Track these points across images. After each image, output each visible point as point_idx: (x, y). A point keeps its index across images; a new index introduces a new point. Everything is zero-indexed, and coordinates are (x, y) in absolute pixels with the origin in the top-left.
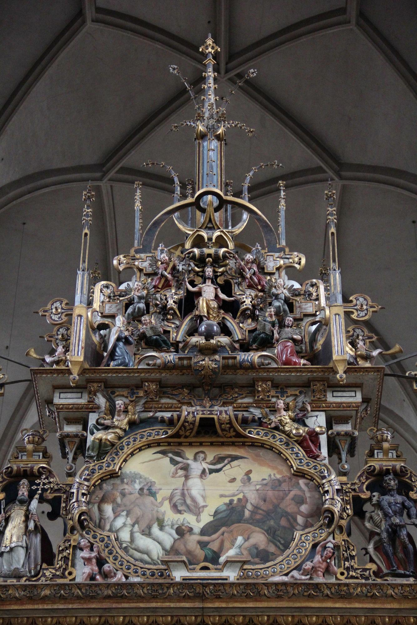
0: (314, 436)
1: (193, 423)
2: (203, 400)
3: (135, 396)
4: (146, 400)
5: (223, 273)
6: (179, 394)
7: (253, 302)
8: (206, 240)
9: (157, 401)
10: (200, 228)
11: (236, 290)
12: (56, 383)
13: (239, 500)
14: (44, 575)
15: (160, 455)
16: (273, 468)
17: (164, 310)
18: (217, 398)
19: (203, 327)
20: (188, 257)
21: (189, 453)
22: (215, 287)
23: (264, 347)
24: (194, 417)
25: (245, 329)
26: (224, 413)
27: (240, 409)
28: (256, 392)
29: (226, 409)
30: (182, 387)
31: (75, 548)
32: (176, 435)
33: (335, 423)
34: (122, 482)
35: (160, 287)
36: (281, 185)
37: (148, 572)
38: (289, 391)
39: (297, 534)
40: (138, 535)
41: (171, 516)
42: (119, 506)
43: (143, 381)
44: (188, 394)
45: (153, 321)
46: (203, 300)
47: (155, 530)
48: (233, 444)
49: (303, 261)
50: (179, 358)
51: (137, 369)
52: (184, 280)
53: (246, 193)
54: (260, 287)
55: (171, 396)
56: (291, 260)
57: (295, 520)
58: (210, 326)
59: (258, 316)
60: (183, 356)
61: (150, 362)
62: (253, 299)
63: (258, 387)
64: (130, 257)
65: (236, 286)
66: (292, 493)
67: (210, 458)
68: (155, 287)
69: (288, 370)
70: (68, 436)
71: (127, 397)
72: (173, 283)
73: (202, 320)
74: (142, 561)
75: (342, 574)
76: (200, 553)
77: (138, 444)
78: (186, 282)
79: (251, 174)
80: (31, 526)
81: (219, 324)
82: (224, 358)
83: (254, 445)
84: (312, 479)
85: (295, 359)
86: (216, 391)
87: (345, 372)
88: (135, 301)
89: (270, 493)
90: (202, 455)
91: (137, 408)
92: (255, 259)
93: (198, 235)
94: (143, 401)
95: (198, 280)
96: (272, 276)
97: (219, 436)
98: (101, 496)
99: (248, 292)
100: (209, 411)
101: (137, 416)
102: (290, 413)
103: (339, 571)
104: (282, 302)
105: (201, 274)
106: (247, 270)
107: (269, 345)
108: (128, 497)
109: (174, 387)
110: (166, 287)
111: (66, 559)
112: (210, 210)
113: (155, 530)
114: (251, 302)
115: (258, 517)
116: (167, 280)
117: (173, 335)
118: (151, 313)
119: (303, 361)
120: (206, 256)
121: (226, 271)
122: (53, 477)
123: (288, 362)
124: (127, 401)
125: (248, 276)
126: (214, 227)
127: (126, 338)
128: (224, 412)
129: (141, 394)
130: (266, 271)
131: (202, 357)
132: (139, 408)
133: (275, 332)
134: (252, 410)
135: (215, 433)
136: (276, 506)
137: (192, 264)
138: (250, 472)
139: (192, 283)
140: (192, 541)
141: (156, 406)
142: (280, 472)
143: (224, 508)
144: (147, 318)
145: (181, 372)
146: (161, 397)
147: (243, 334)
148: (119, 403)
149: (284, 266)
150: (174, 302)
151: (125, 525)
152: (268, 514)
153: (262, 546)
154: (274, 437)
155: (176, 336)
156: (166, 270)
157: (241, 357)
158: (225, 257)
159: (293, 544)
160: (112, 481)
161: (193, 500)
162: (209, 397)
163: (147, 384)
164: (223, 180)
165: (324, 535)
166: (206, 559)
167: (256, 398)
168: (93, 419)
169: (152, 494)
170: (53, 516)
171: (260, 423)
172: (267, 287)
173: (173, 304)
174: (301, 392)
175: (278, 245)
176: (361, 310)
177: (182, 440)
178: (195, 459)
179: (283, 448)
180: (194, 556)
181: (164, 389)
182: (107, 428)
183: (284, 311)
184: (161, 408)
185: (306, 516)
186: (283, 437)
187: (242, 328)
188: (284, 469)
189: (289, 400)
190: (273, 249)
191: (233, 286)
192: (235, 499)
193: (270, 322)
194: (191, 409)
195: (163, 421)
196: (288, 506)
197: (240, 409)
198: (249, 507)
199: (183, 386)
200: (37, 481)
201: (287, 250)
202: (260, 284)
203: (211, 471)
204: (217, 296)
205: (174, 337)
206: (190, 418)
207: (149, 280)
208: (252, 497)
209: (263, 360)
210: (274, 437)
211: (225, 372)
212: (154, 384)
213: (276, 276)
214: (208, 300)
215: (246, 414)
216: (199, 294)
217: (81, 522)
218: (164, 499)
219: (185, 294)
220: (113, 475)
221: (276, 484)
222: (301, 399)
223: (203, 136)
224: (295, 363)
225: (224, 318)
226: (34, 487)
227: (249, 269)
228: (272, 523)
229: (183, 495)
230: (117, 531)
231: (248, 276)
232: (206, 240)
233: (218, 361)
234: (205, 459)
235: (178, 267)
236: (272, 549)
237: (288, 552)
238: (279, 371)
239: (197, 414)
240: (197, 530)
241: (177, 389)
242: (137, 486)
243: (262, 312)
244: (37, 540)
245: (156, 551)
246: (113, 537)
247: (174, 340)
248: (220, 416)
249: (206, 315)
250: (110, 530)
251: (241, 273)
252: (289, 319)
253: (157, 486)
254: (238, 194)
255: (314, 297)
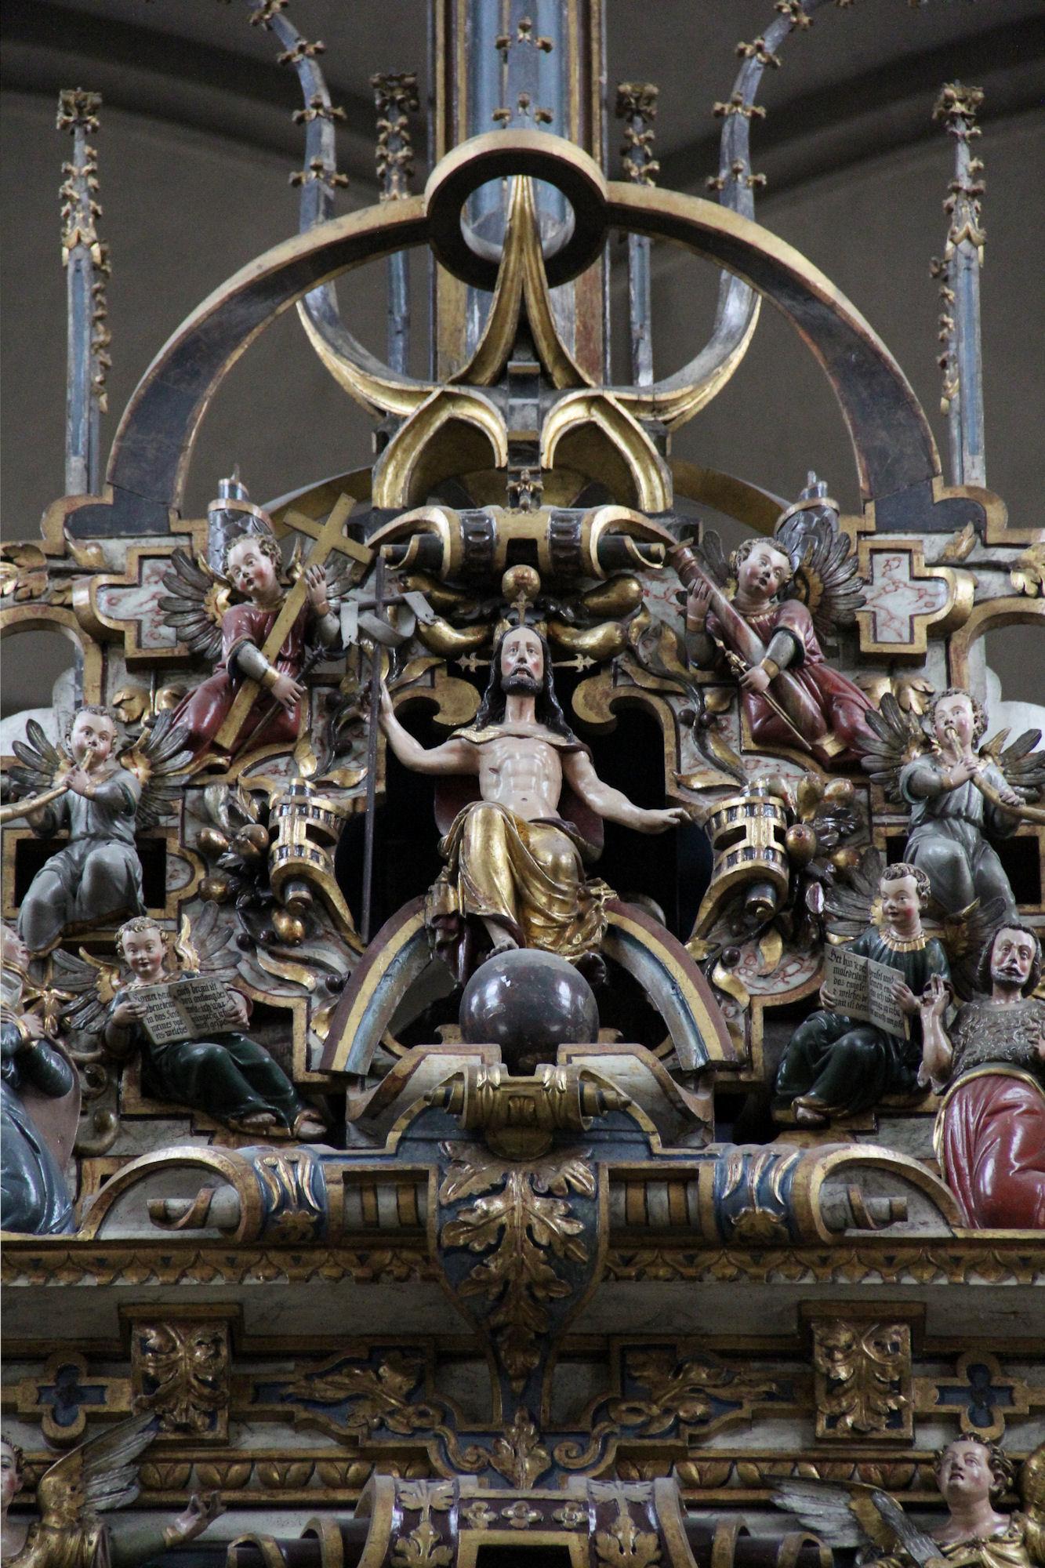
2: (498, 1436)
3: (82, 1411)
4: (150, 1436)
5: (603, 659)
7: (791, 837)
8: (502, 457)
9: (215, 1444)
18: (585, 1424)
19: (492, 990)
20: (393, 560)
22: (561, 741)
23: (861, 1113)
24: (445, 1540)
25: (744, 1000)
26: (625, 1519)
27: (722, 1495)
28: (821, 1389)
30: (371, 1362)
35: (227, 740)
38: (1020, 1388)
44: (408, 1398)
45: (189, 953)
46: (488, 822)
50: (352, 1180)
51: (96, 1243)
52: (368, 700)
54: (830, 747)
55: (302, 1414)
56: (1020, 580)
60: (370, 1165)
61: (176, 1203)
62: (791, 819)
63: (830, 1356)
64: (37, 561)
65: (688, 735)
68: (195, 742)
69: (1014, 1254)
72: (307, 720)
73: (482, 947)
78: (381, 710)
81: (586, 967)
82: (620, 1179)
88: (79, 828)
91: (96, 1485)
92: (799, 574)
93: (454, 424)
94: (132, 1444)
96: (905, 676)
99: (762, 772)
100: (534, 1503)
101: (94, 1537)
104: (971, 833)
105: (473, 663)
106: (755, 640)
107: (892, 1101)
110: (264, 742)
114: (780, 835)
118: (172, 899)
120: (501, 551)
121: (631, 651)
125: (760, 676)
126: (545, 374)
128: (624, 1511)
129: (122, 1398)
130: (866, 645)
131: (491, 1174)
133: (929, 1020)
134: (795, 1500)
137: (416, 600)
144: (152, 934)
145: (362, 1261)
146: (239, 1419)
147: (733, 1031)
149: (977, 617)
150: (312, 833)
155: (330, 1044)
156: (260, 642)
162: (533, 1419)
163: (153, 1338)
167: (821, 1427)
172: (877, 745)
173: (310, 845)
175: (937, 483)
181: (264, 1371)
183: (985, 890)
184: (242, 1484)
187: (727, 997)
191: (669, 735)
194: (426, 1494)
197: (722, 1495)
201: (996, 513)
202: (831, 724)
204: (570, 800)
205: (317, 1045)
207: (161, 701)
209: (856, 1196)
211: (628, 1262)
212: (199, 1334)
213: (933, 675)
214: (521, 825)
219: (381, 787)
225: (614, 933)
231: (760, 676)
232: (502, 457)
233: (583, 1196)
238: (957, 1261)
239: (464, 1523)
241: (337, 1369)
243: (850, 898)
247: (316, 1063)
248: (603, 1538)
249: (506, 911)
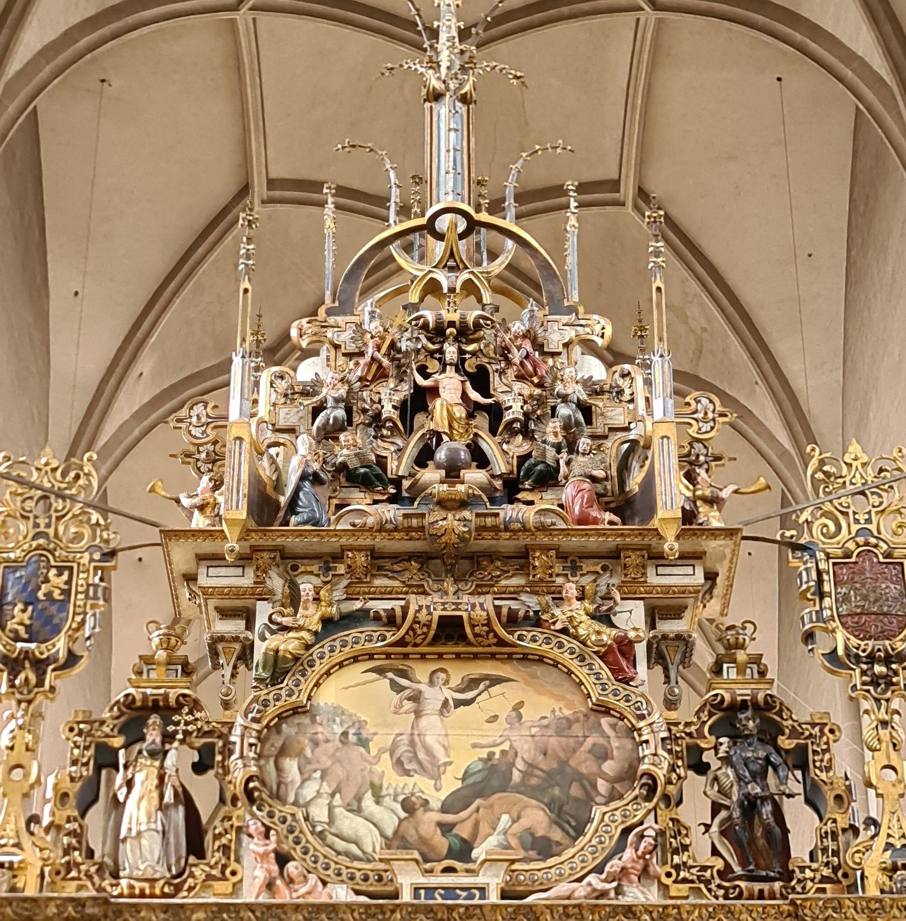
0: (625, 646)
1: (428, 625)
2: (443, 581)
3: (331, 573)
4: (349, 581)
5: (474, 354)
6: (404, 570)
7: (525, 408)
8: (445, 290)
9: (367, 583)
10: (435, 267)
11: (496, 383)
12: (200, 551)
13: (503, 752)
14: (192, 875)
15: (374, 676)
16: (560, 698)
17: (377, 420)
18: (467, 578)
19: (443, 453)
20: (416, 325)
21: (422, 671)
22: (462, 379)
23: (542, 486)
24: (430, 614)
25: (511, 454)
26: (478, 608)
27: (504, 596)
28: (531, 567)
29: (482, 599)
30: (409, 560)
31: (239, 830)
32: (401, 643)
33: (660, 619)
34: (313, 721)
35: (369, 378)
36: (570, 187)
37: (358, 875)
38: (584, 566)
39: (597, 812)
40: (340, 811)
41: (393, 781)
42: (309, 761)
43: (344, 549)
44: (419, 570)
45: (359, 441)
46: (442, 405)
47: (368, 802)
48: (493, 656)
49: (608, 332)
50: (405, 516)
51: (335, 530)
52: (409, 366)
53: (512, 201)
54: (536, 380)
55: (390, 574)
56: (588, 330)
57: (594, 786)
58: (454, 452)
59: (533, 431)
60: (410, 512)
61: (357, 521)
62: (525, 402)
63: (534, 559)
64: (318, 323)
65: (497, 375)
66: (590, 741)
67: (455, 681)
68: (361, 379)
69: (584, 533)
70: (222, 639)
71: (318, 575)
72: (392, 372)
73: (439, 441)
74: (347, 854)
75: (669, 875)
76: (442, 843)
77: (338, 657)
78: (412, 369)
79: (519, 165)
80: (169, 797)
81: (468, 446)
83: (526, 658)
84: (622, 718)
85: (594, 513)
86: (465, 565)
87: (678, 538)
88: (329, 405)
89: (554, 741)
90: (442, 676)
91: (335, 594)
92: (528, 331)
93: (432, 279)
94: (345, 582)
95: (433, 365)
96: (556, 358)
97: (470, 644)
98: (279, 744)
99: (518, 386)
100: (454, 604)
101: (335, 609)
102: (587, 605)
103: (661, 871)
104: (574, 405)
105: (438, 356)
106: (516, 350)
107: (551, 482)
108: (323, 746)
109: (396, 557)
110: (380, 378)
111: (226, 849)
112: (452, 237)
113: (368, 802)
114: (522, 407)
115: (534, 781)
116: (380, 366)
117: (392, 465)
118: (354, 424)
119: (608, 516)
120: (446, 324)
121: (481, 350)
122: (201, 709)
123: (583, 519)
124: (317, 581)
125: (517, 360)
126: (458, 265)
127: (315, 474)
128: (478, 605)
129: (341, 569)
130: (546, 349)
131: (443, 514)
132: (338, 594)
133: (562, 462)
134: (524, 597)
135: (463, 638)
136: (564, 763)
137: (422, 337)
138: (521, 704)
139: (423, 371)
140: (428, 821)
141: (366, 590)
142: (569, 705)
143: (480, 766)
144: (350, 437)
145: (407, 535)
146: (374, 576)
147: (508, 463)
148: (306, 587)
149: (576, 340)
150: (394, 407)
151: (319, 794)
152: (550, 775)
153: (540, 833)
154: (560, 645)
155: (398, 467)
156: (379, 350)
157: (506, 513)
158: (478, 326)
159: (590, 829)
160: (297, 720)
161: (429, 752)
162: (453, 576)
163: (350, 555)
164: (473, 175)
165: (640, 814)
166: (451, 854)
167: (531, 578)
168: (263, 611)
169: (363, 742)
170: (200, 768)
171: (537, 622)
172: (549, 380)
173: (393, 410)
174: (605, 568)
175: (565, 300)
176: (705, 420)
177: (409, 649)
178: (431, 683)
179: (574, 665)
180: (432, 848)
181: (380, 562)
182: (285, 629)
183: (578, 423)
184: (374, 593)
185: (613, 781)
186: (575, 644)
187: (507, 453)
188: (577, 699)
189: (586, 580)
190: (557, 307)
191: (491, 375)
192: (497, 750)
193: (553, 445)
194: (424, 601)
195: (377, 618)
196: (584, 763)
197: (504, 596)
198: (520, 764)
199: (411, 556)
200: (176, 718)
201: (581, 310)
202: (536, 373)
203: (459, 703)
204: (464, 396)
205: (394, 468)
206: (423, 616)
207: (351, 365)
208: (526, 750)
209: (542, 519)
210: (560, 645)
211: (479, 535)
212: (363, 553)
213: (563, 359)
214: (451, 405)
215: (514, 605)
216: (434, 391)
217: (249, 793)
218: (381, 751)
219: (412, 391)
220: (297, 711)
221: (564, 726)
222: (604, 580)
223: (437, 96)
224: (595, 521)
225: (476, 435)
226: (171, 728)
227: (519, 349)
228: (557, 791)
229: (412, 743)
230: (307, 805)
231: (517, 360)
232: (445, 290)
233: (468, 520)
234: (446, 682)
235: (399, 345)
236: (557, 835)
237: (582, 841)
238: (568, 534)
239: (435, 609)
240: (435, 804)
241: (399, 562)
242: (339, 730)
243: (541, 425)
244: (179, 815)
245: (371, 841)
246: (300, 816)
247: (394, 472)
248: (472, 613)
249: (447, 430)
250: (295, 804)
251: (504, 352)
252: (584, 443)
253: (370, 729)
254: (496, 207)
255: (626, 397)
